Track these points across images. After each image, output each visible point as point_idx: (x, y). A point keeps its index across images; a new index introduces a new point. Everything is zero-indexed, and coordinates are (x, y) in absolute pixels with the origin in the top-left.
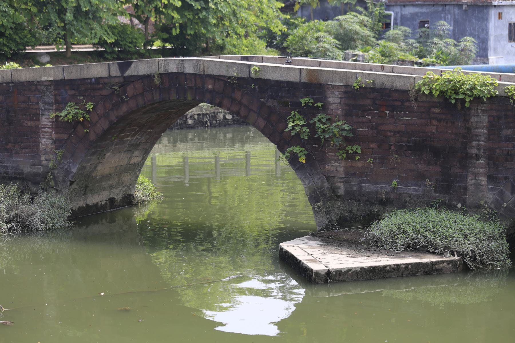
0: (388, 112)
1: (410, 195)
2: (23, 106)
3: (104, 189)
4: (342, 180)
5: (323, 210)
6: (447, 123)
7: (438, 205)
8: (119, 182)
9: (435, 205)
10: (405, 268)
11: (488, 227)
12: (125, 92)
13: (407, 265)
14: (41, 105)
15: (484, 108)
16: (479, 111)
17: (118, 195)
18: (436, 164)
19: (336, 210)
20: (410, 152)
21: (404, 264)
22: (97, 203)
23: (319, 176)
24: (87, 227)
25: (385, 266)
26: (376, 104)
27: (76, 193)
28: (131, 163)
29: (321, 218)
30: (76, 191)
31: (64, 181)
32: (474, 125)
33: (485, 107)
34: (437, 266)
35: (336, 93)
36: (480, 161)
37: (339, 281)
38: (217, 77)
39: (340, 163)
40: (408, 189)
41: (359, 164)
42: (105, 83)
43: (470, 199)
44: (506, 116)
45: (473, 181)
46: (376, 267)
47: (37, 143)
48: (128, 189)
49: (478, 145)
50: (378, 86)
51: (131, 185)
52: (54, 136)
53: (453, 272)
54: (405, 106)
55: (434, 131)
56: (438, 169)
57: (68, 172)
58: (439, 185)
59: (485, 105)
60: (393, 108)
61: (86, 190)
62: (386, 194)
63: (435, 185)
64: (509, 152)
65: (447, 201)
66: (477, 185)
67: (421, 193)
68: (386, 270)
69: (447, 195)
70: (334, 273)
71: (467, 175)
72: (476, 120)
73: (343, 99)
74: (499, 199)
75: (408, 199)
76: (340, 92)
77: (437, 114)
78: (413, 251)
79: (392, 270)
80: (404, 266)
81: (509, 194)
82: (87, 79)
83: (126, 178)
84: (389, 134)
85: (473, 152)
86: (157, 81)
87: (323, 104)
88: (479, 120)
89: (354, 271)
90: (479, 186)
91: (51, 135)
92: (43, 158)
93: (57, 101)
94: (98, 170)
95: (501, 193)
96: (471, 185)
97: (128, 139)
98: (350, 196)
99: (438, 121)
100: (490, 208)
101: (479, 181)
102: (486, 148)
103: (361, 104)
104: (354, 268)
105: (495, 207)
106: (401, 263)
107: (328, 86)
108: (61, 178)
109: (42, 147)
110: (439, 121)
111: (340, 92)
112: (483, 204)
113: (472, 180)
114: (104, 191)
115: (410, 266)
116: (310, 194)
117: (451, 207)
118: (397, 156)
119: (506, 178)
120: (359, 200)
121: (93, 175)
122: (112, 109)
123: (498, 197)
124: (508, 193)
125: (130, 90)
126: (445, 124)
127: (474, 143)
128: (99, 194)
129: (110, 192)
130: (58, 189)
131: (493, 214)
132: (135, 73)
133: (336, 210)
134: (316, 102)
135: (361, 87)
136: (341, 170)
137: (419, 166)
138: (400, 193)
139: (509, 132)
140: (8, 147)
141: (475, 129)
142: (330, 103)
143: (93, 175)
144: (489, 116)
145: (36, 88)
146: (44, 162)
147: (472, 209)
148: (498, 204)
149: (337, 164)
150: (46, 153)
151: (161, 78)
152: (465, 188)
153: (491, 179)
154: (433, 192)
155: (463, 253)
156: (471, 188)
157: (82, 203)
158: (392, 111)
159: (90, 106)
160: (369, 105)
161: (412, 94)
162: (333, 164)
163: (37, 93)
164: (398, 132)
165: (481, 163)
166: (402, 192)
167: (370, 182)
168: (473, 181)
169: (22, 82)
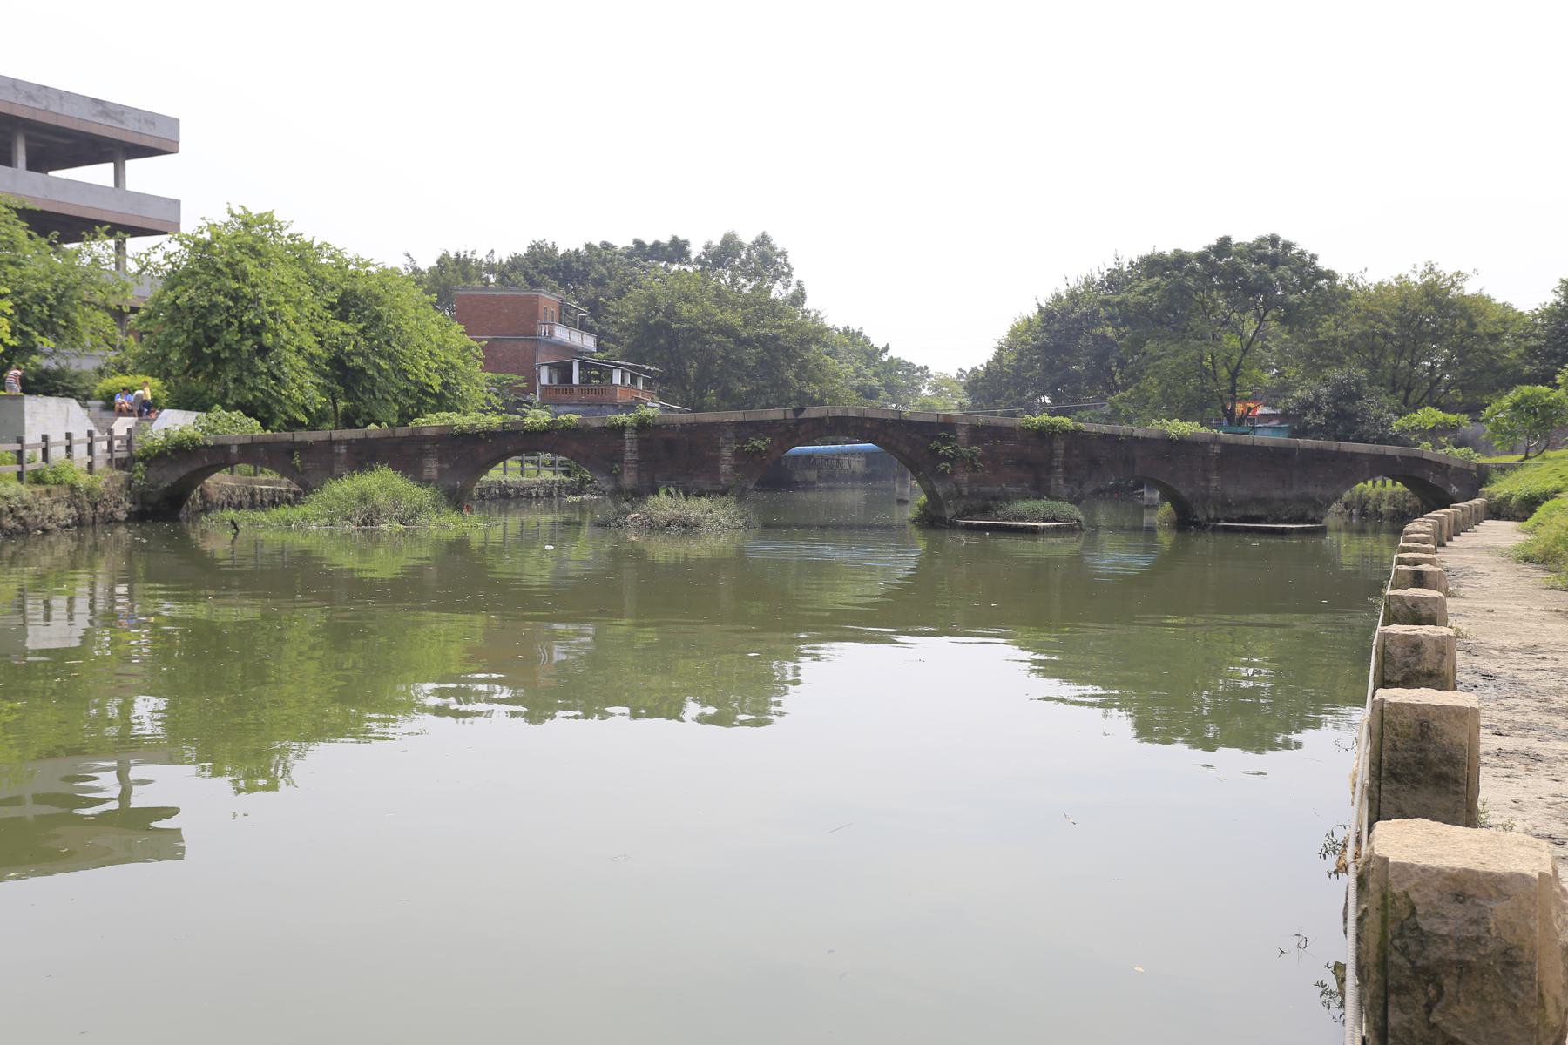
14: (722, 440)
40: (1011, 489)
43: (1052, 493)
52: (733, 462)
66: (1057, 485)
92: (722, 479)
93: (737, 437)
95: (1072, 489)
98: (972, 495)
109: (722, 471)
124: (1076, 488)
136: (966, 478)
139: (1077, 452)
146: (723, 482)
148: (1070, 495)
152: (1050, 487)
153: (1066, 480)
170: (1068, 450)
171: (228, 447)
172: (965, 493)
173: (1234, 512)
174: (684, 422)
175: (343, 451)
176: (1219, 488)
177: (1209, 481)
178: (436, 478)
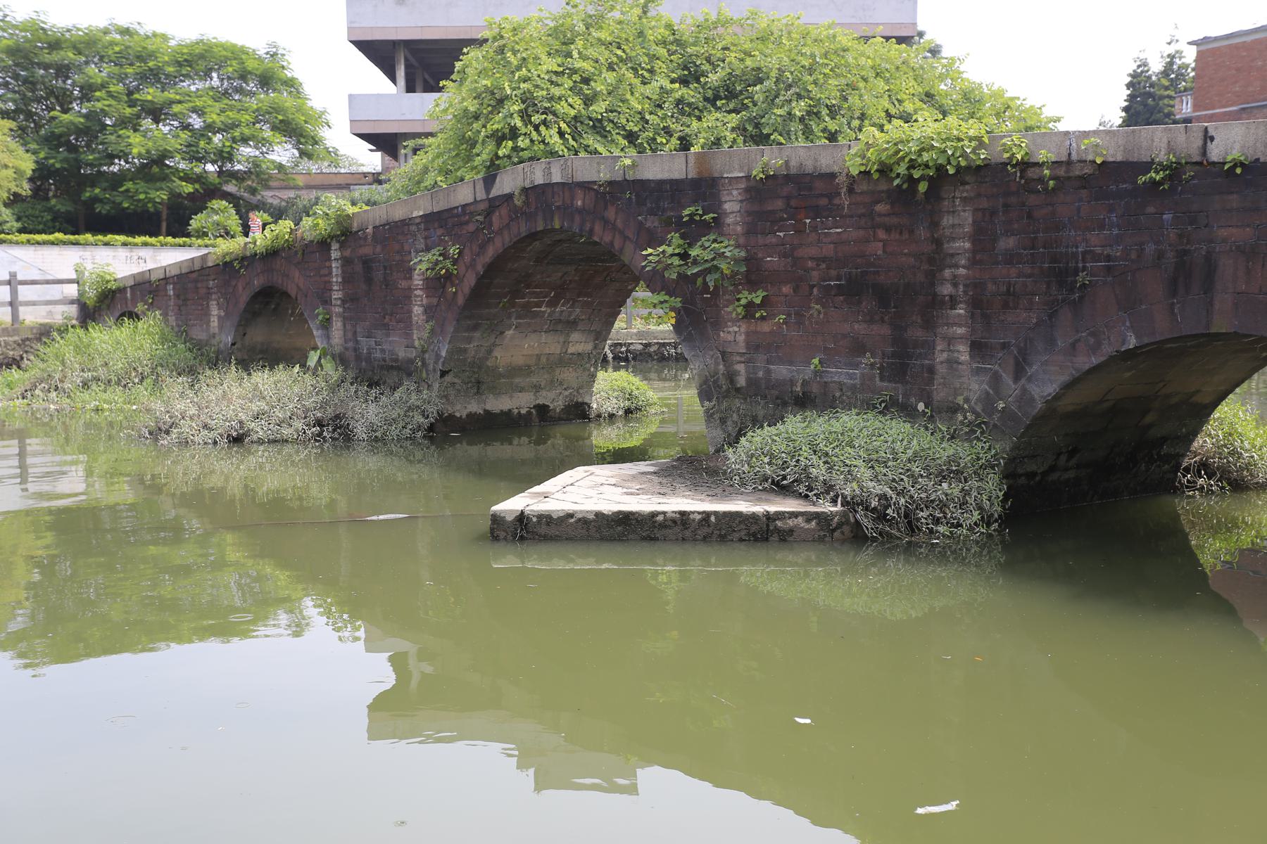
0: (808, 221)
1: (841, 386)
2: (397, 258)
4: (743, 359)
5: (717, 416)
6: (901, 233)
7: (883, 405)
8: (552, 381)
9: (878, 406)
10: (701, 521)
11: (963, 452)
12: (491, 225)
13: (707, 514)
15: (965, 194)
16: (957, 202)
17: (555, 400)
18: (883, 321)
19: (735, 416)
20: (841, 298)
21: (699, 513)
22: (510, 410)
23: (711, 353)
25: (654, 515)
26: (791, 207)
27: (459, 390)
28: (570, 351)
29: (714, 431)
30: (457, 387)
31: (434, 370)
32: (947, 232)
33: (967, 191)
34: (779, 523)
35: (735, 193)
36: (957, 311)
37: (546, 538)
38: (586, 185)
39: (739, 327)
40: (840, 374)
41: (766, 327)
42: (471, 213)
43: (940, 394)
44: (1006, 205)
45: (945, 355)
46: (631, 513)
47: (410, 312)
48: (575, 393)
49: (955, 276)
50: (793, 171)
51: (581, 387)
52: (425, 301)
53: (821, 540)
54: (836, 205)
55: (880, 252)
56: (886, 330)
57: (438, 356)
58: (887, 363)
60: (816, 212)
62: (805, 383)
63: (882, 365)
64: (1010, 287)
65: (901, 396)
66: (952, 363)
67: (857, 381)
68: (656, 522)
69: (899, 385)
70: (535, 520)
71: (934, 340)
72: (951, 222)
73: (745, 203)
74: (991, 392)
75: (838, 394)
76: (740, 191)
77: (885, 215)
78: (776, 491)
79: (670, 523)
80: (699, 517)
81: (1011, 383)
82: (455, 208)
83: (569, 375)
84: (810, 264)
85: (946, 292)
86: (518, 202)
87: (716, 215)
88: (956, 222)
89: (579, 520)
90: (955, 365)
91: (422, 301)
94: (496, 358)
95: (996, 380)
96: (942, 363)
97: (542, 309)
99: (887, 230)
100: (974, 412)
101: (956, 355)
102: (968, 282)
103: (769, 209)
105: (983, 410)
106: (692, 510)
107: (723, 180)
108: (431, 367)
110: (888, 229)
111: (740, 191)
112: (961, 403)
113: (942, 351)
114: (520, 392)
115: (713, 518)
116: (701, 386)
117: (908, 412)
118: (818, 307)
119: (1004, 346)
120: (766, 397)
121: (489, 363)
122: (478, 255)
123: (990, 387)
124: (1007, 379)
125: (495, 218)
126: (898, 236)
127: (947, 273)
128: (511, 397)
129: (535, 395)
130: (430, 382)
131: (979, 426)
132: (500, 193)
133: (735, 415)
134: (704, 214)
135: (768, 177)
136: (741, 338)
137: (856, 326)
138: (826, 383)
140: (386, 321)
141: (948, 242)
142: (726, 214)
143: (489, 363)
144: (976, 210)
145: (409, 230)
147: (943, 415)
148: (988, 402)
149: (736, 329)
150: (419, 328)
151: (526, 196)
152: (931, 370)
153: (978, 348)
154: (877, 379)
155: (852, 499)
156: (941, 370)
157: (474, 407)
158: (813, 219)
159: (453, 250)
160: (781, 210)
161: (841, 179)
162: (731, 329)
163: (409, 236)
164: (824, 259)
165: (960, 315)
166: (830, 380)
167: (781, 361)
168: (945, 355)
169: (396, 222)
170: (982, 237)
171: (125, 288)
172: (742, 381)
174: (377, 224)
175: (171, 293)
178: (216, 330)
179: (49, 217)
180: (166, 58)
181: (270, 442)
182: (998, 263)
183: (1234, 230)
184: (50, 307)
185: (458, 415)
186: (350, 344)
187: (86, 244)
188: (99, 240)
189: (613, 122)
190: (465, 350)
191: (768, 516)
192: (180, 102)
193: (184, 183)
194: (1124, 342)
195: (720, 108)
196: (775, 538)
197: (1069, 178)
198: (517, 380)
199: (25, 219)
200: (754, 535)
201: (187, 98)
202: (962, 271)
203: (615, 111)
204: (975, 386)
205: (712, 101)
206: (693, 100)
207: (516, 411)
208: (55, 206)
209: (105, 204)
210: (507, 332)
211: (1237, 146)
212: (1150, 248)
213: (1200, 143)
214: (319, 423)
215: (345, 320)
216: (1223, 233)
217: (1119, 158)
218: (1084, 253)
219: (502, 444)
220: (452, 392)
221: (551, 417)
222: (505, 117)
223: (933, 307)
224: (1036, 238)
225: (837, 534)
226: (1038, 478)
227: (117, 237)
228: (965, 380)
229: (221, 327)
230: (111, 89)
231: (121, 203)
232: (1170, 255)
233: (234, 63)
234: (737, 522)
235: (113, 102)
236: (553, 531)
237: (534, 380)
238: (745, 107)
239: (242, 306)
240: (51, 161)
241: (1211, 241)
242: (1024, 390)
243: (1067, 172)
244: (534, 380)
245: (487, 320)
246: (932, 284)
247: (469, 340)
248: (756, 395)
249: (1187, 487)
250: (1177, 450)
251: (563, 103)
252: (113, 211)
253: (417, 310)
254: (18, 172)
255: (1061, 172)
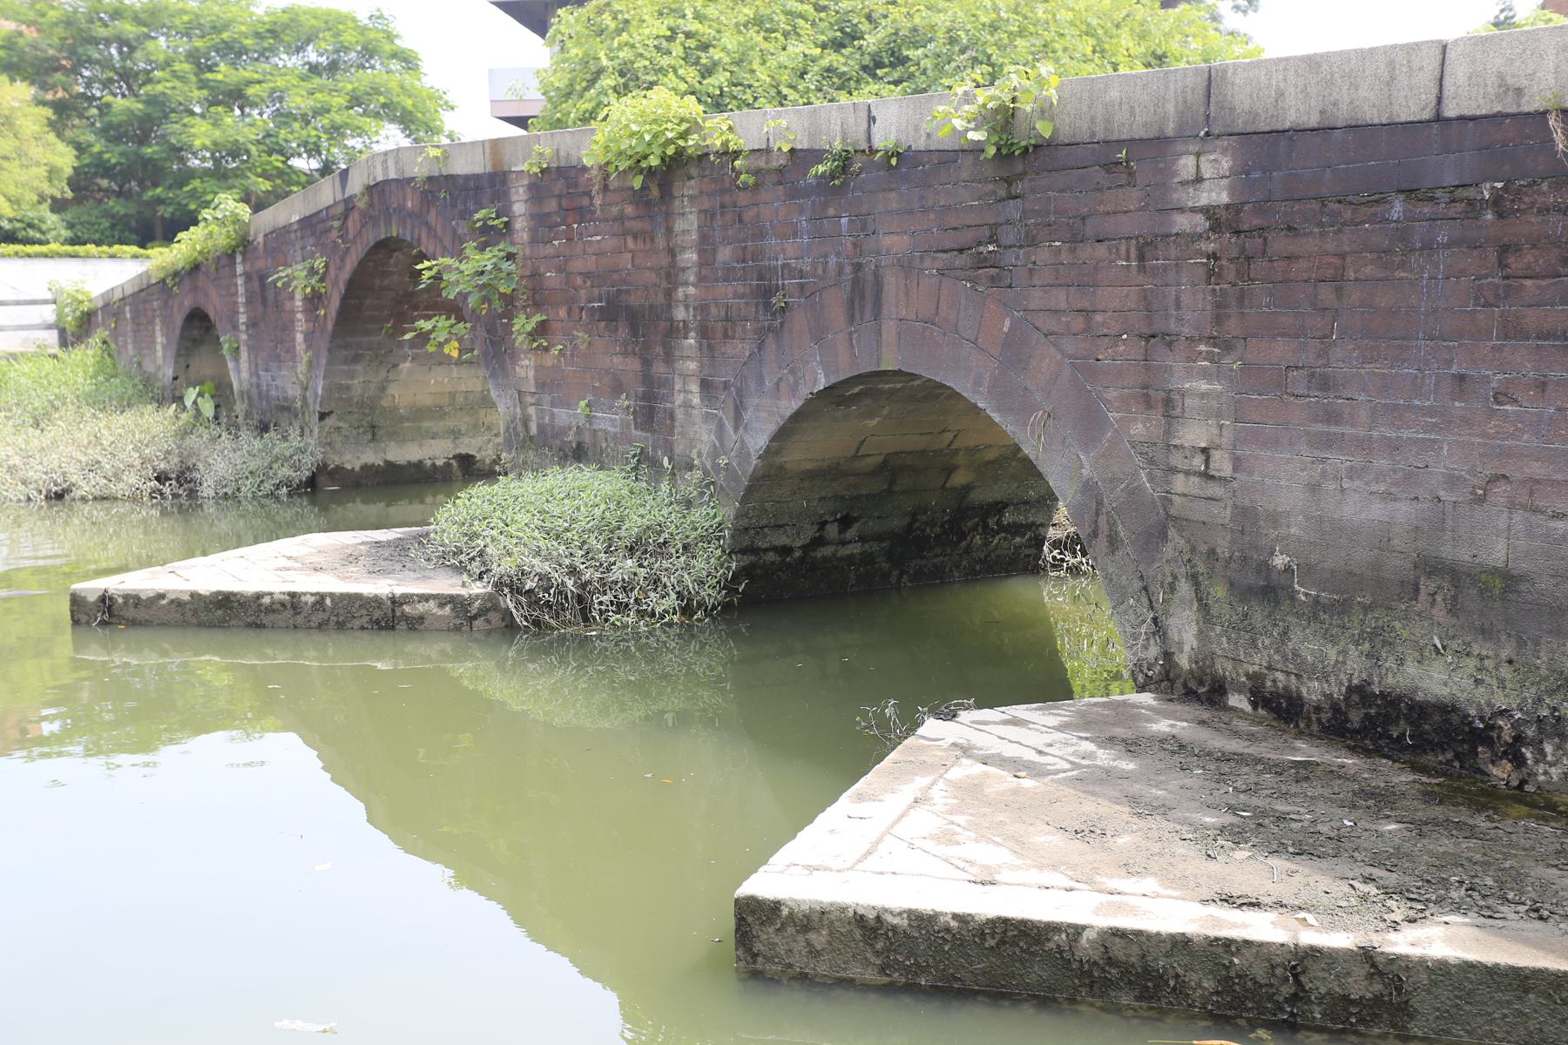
3: (434, 436)
8: (475, 426)
10: (314, 604)
21: (312, 594)
22: (420, 462)
24: (388, 505)
27: (346, 436)
34: (407, 608)
37: (134, 623)
44: (723, 206)
46: (234, 594)
49: (686, 296)
50: (563, 164)
53: (458, 629)
55: (629, 266)
57: (316, 393)
59: (692, 182)
61: (374, 433)
66: (687, 405)
68: (261, 605)
70: (120, 600)
75: (604, 445)
79: (278, 606)
80: (311, 600)
89: (172, 601)
94: (393, 396)
104: (174, 591)
115: (328, 601)
121: (385, 403)
124: (729, 427)
125: (350, 224)
128: (421, 445)
129: (453, 442)
131: (707, 486)
135: (543, 171)
143: (385, 403)
153: (706, 385)
156: (680, 415)
157: (372, 457)
158: (579, 224)
159: (319, 263)
170: (706, 245)
173: (1308, 644)
175: (128, 316)
176: (1222, 464)
177: (1168, 407)
179: (107, 224)
180: (243, 28)
181: (95, 499)
182: (717, 280)
183: (894, 238)
184: (24, 334)
185: (349, 467)
186: (254, 380)
187: (88, 256)
188: (104, 252)
189: (735, 98)
190: (348, 388)
191: (395, 601)
192: (259, 82)
193: (261, 180)
194: (815, 383)
195: (881, 78)
196: (403, 625)
197: (768, 171)
198: (426, 424)
199: (79, 227)
200: (377, 622)
201: (269, 77)
202: (691, 290)
203: (741, 85)
204: (705, 437)
205: (871, 69)
206: (845, 69)
207: (429, 463)
208: (113, 207)
209: (170, 204)
210: (402, 366)
211: (894, 129)
212: (833, 260)
213: (864, 125)
214: (161, 478)
215: (250, 348)
216: (887, 241)
217: (805, 146)
218: (784, 266)
219: (411, 503)
220: (337, 438)
221: (478, 470)
222: (599, 94)
223: (674, 332)
224: (745, 247)
225: (477, 623)
226: (797, 554)
227: (125, 248)
228: (696, 428)
229: (164, 357)
230: (176, 68)
231: (187, 205)
232: (848, 269)
233: (328, 35)
234: (357, 605)
235: (178, 84)
236: (141, 615)
237: (450, 423)
238: (911, 76)
239: (178, 331)
240: (106, 156)
241: (878, 253)
242: (743, 441)
243: (767, 162)
244: (450, 423)
245: (370, 349)
246: (669, 307)
247: (352, 375)
248: (544, 445)
249: (1053, 566)
250: (1031, 519)
251: (671, 75)
252: (178, 213)
253: (299, 337)
254: (52, 172)
255: (762, 164)
